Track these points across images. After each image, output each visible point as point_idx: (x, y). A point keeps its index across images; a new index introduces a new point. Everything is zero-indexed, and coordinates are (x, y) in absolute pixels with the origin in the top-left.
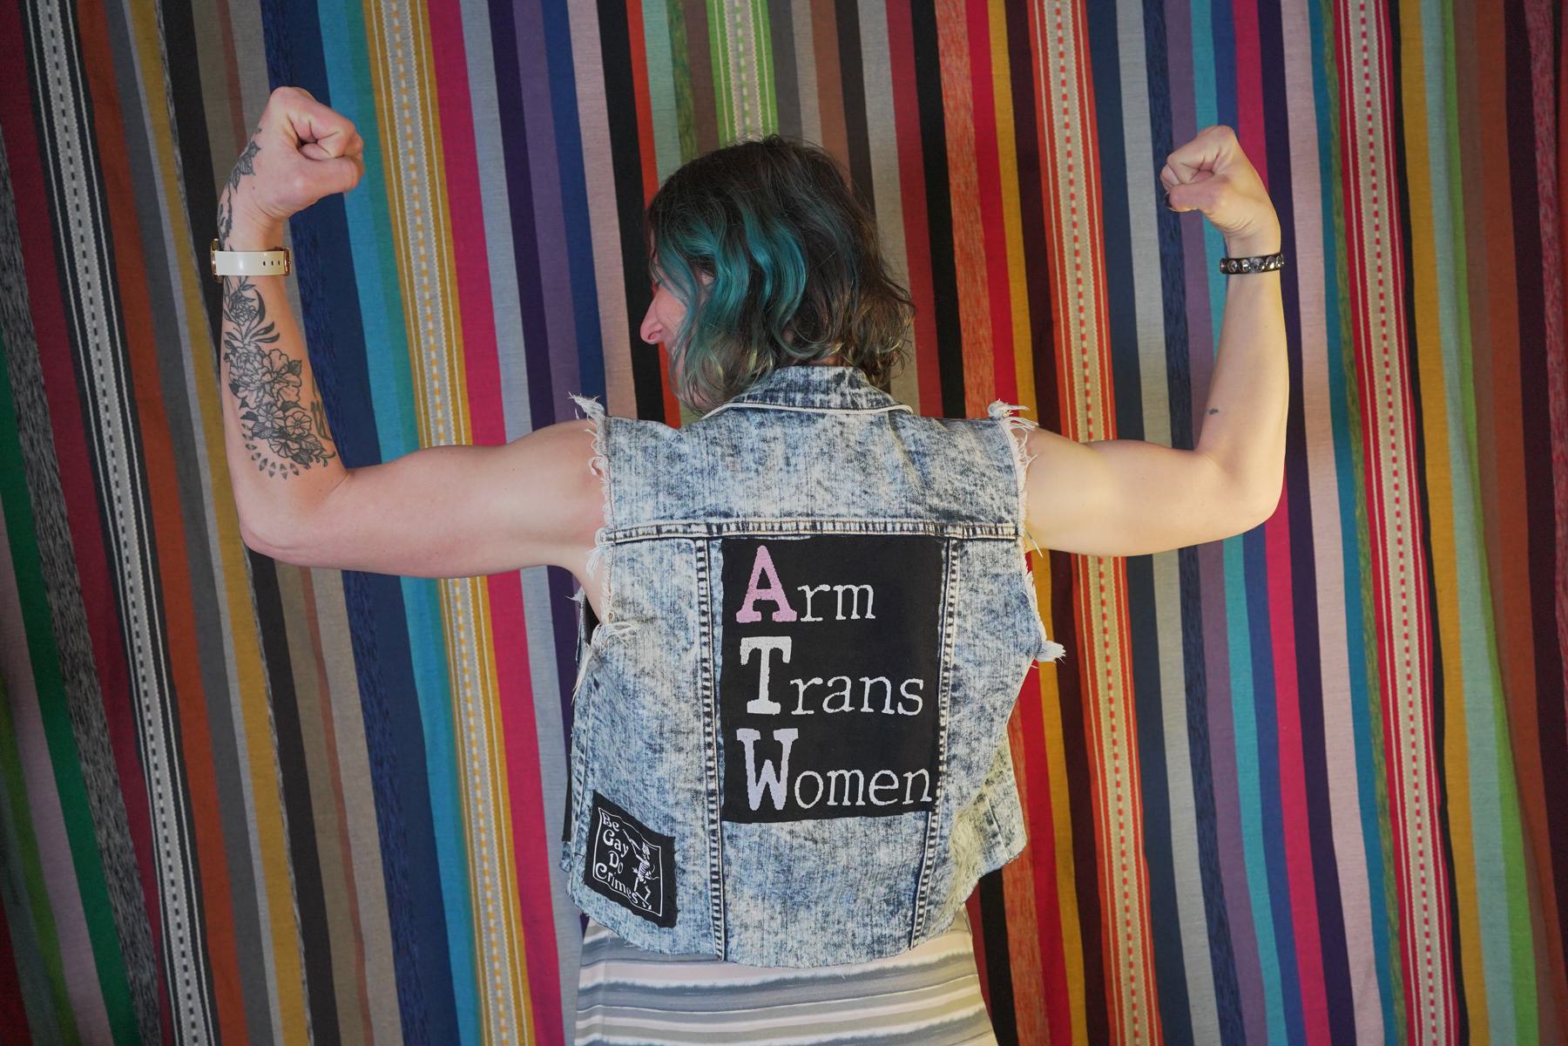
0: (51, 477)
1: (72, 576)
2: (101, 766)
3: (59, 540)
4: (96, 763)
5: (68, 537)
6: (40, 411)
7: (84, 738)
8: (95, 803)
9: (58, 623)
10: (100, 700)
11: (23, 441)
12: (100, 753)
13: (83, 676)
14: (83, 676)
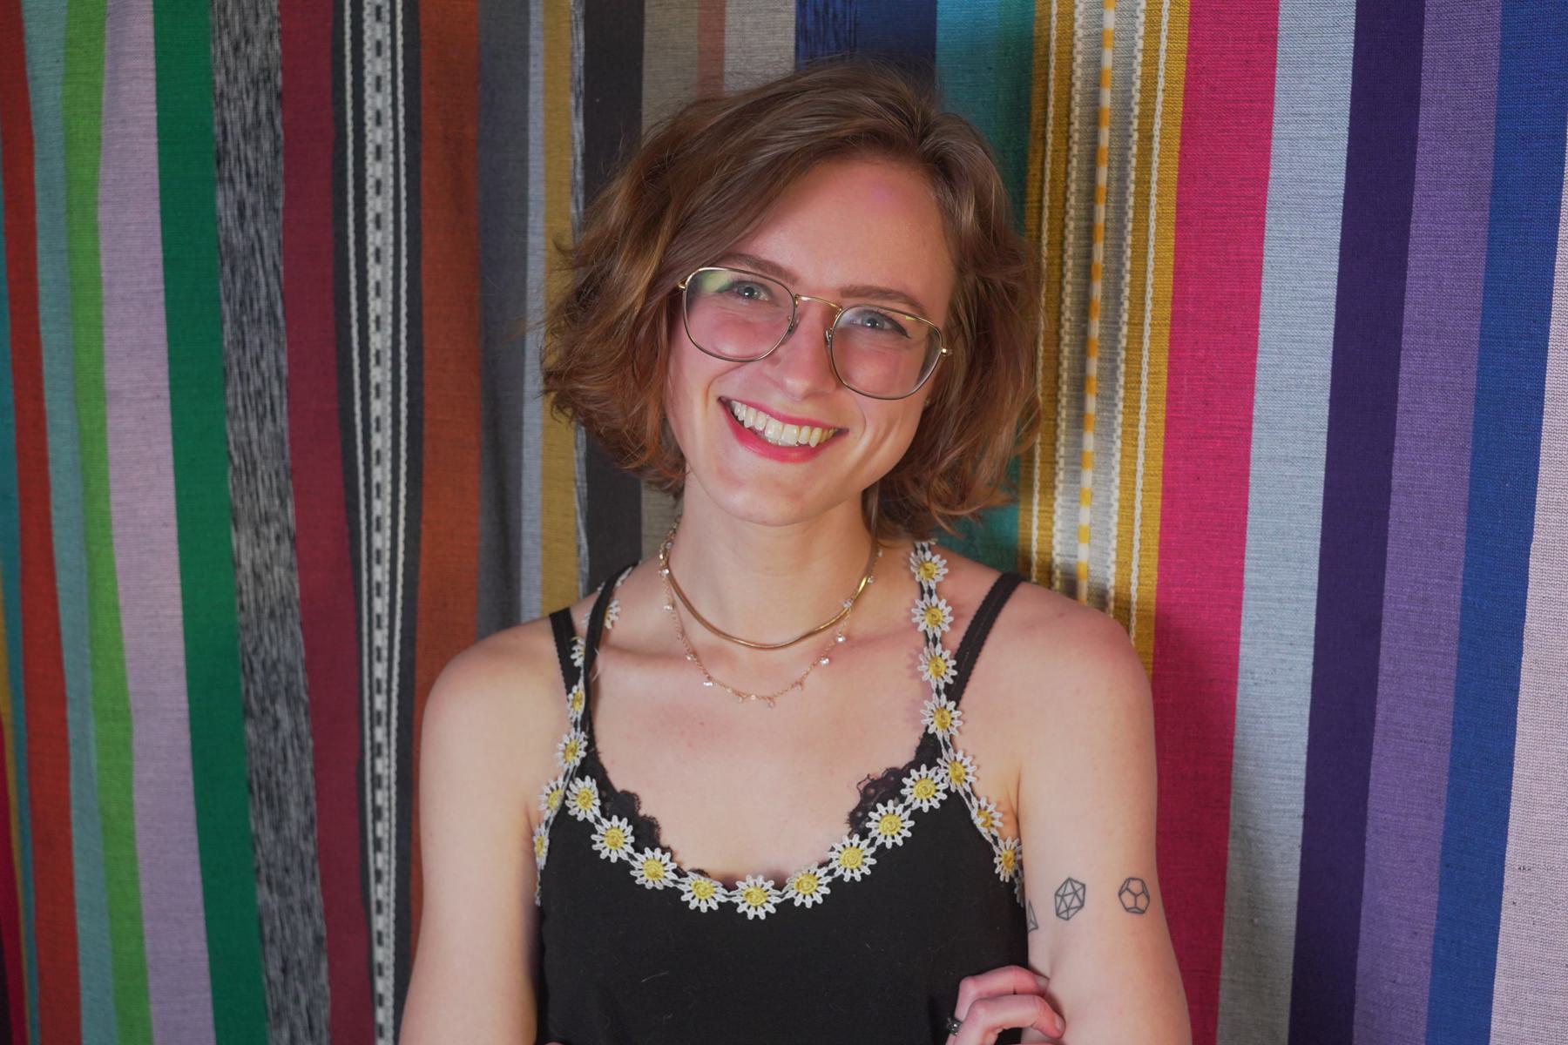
0: (267, 286)
1: (283, 504)
2: (295, 901)
3: (269, 425)
4: (284, 892)
5: (283, 422)
6: (266, 146)
7: (268, 836)
8: (275, 974)
9: (248, 599)
10: (308, 765)
11: (224, 204)
12: (296, 874)
13: (281, 711)
14: (281, 711)
